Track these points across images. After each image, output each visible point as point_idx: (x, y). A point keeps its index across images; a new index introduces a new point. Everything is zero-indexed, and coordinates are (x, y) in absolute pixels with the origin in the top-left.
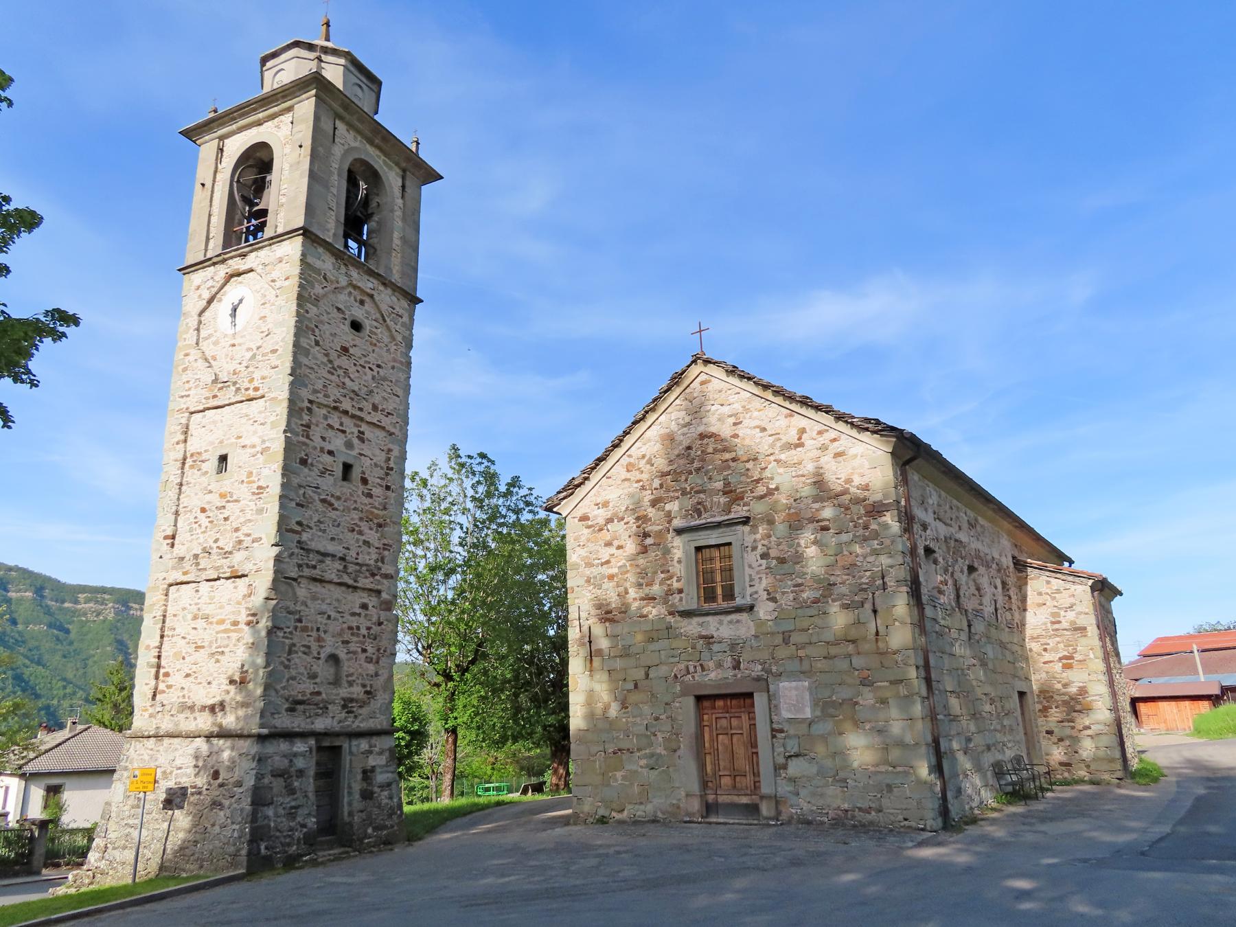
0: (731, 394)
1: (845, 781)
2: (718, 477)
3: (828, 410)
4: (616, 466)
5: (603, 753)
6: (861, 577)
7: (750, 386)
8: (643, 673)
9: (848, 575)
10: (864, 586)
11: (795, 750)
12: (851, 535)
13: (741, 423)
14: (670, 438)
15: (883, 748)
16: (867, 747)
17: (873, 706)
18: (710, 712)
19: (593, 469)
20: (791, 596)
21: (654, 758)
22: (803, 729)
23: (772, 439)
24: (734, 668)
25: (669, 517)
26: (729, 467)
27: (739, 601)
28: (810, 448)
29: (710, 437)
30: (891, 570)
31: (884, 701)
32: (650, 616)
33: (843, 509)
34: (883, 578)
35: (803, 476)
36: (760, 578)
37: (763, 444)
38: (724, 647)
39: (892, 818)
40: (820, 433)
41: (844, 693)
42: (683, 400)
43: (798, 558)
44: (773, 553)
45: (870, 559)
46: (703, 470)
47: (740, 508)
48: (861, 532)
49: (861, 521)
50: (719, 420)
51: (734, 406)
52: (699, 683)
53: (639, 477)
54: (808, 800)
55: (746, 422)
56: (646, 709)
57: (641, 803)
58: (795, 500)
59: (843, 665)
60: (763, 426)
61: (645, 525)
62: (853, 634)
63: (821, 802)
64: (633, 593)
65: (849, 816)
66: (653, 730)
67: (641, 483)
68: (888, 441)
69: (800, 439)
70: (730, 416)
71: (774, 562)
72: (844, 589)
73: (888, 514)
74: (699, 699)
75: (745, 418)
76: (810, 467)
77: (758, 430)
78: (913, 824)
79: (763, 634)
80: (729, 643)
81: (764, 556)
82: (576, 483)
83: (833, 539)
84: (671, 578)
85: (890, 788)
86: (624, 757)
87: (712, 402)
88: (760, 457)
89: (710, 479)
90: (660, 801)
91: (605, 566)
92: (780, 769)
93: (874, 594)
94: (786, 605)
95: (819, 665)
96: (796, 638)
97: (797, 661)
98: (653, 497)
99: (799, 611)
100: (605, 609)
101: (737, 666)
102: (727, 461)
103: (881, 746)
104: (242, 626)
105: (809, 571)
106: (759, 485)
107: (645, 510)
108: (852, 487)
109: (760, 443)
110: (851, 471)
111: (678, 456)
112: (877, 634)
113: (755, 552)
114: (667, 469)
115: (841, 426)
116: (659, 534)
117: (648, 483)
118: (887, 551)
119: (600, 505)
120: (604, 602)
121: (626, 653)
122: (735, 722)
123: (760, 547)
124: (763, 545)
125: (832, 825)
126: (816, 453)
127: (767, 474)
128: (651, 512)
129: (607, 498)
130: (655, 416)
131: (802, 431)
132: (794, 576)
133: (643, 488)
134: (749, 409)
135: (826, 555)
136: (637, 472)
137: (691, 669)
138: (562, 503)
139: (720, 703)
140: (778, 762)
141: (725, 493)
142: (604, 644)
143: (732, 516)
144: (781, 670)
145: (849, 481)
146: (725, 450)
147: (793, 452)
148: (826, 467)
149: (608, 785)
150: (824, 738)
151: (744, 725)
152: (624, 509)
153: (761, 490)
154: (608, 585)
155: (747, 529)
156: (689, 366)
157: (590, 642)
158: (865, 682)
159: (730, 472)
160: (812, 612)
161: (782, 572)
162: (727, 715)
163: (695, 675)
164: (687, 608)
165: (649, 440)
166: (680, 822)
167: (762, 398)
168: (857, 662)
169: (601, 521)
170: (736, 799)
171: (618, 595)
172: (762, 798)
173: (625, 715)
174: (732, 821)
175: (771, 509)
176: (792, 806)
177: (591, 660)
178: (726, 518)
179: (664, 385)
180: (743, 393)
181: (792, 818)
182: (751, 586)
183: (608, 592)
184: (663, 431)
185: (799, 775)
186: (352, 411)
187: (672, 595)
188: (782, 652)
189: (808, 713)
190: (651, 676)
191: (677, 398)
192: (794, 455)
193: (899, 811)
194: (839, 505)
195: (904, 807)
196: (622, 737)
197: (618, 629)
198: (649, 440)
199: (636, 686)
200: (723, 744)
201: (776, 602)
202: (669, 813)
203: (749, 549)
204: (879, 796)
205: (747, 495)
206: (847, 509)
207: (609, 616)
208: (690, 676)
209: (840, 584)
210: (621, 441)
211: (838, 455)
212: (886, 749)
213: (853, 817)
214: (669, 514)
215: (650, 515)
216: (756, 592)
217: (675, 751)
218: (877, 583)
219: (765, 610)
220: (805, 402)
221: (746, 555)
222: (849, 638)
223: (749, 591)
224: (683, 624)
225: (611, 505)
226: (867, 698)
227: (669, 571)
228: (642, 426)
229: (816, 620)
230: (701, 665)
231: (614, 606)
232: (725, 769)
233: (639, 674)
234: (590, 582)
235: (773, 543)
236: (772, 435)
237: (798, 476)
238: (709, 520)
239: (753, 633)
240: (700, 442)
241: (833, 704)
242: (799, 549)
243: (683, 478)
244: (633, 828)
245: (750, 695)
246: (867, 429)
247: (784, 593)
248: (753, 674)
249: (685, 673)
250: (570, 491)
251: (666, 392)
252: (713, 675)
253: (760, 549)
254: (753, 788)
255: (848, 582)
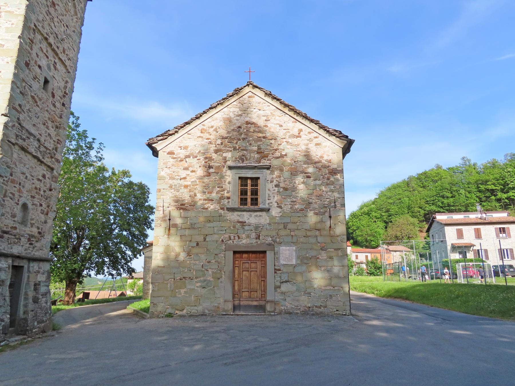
0: (265, 106)
1: (310, 293)
2: (255, 144)
3: (317, 123)
4: (195, 129)
5: (173, 280)
6: (324, 201)
7: (277, 104)
8: (203, 238)
9: (318, 199)
10: (326, 205)
11: (286, 279)
12: (321, 182)
13: (269, 120)
14: (229, 120)
15: (329, 279)
16: (322, 278)
17: (326, 259)
18: (239, 260)
19: (182, 127)
20: (290, 206)
21: (205, 283)
22: (291, 269)
23: (285, 131)
24: (256, 239)
25: (225, 160)
26: (261, 141)
27: (261, 206)
28: (304, 139)
29: (252, 124)
30: (339, 200)
31: (331, 258)
32: (209, 209)
33: (318, 169)
34: (335, 203)
35: (299, 151)
36: (274, 196)
37: (280, 133)
38: (252, 228)
39: (331, 310)
40: (309, 133)
41: (313, 253)
42: (238, 103)
43: (294, 189)
44: (282, 185)
45: (330, 193)
46: (247, 140)
47: (266, 161)
48: (326, 181)
49: (326, 176)
50: (258, 117)
51: (266, 112)
52: (236, 245)
53: (208, 137)
54: (290, 303)
55: (272, 121)
56: (203, 257)
57: (196, 306)
58: (295, 162)
59: (312, 240)
60: (281, 124)
61: (210, 162)
62: (319, 226)
63: (297, 304)
64: (199, 196)
65: (311, 310)
66: (206, 268)
67: (210, 140)
68: (343, 142)
69: (299, 134)
70: (263, 116)
71: (282, 190)
72: (316, 206)
73: (339, 175)
74: (235, 253)
75: (271, 118)
76: (303, 148)
77: (278, 126)
78: (341, 313)
79: (273, 223)
80: (255, 226)
81: (276, 186)
82: (170, 133)
83: (312, 183)
84: (224, 190)
85: (331, 296)
86: (187, 282)
87: (255, 107)
88: (278, 139)
89: (250, 144)
90: (207, 304)
91: (183, 180)
92: (277, 288)
93: (330, 209)
94: (287, 210)
95: (301, 240)
96: (290, 226)
97: (290, 237)
98: (216, 148)
99: (293, 214)
100: (181, 203)
101: (258, 237)
102: (260, 137)
103: (328, 278)
104: (96, 149)
105: (299, 195)
106: (277, 152)
107: (211, 155)
108: (323, 160)
109: (278, 132)
110: (323, 153)
111: (233, 130)
112: (330, 227)
113: (272, 184)
114: (225, 135)
115: (321, 132)
116: (218, 168)
117: (214, 141)
118: (337, 191)
119: (182, 148)
120: (180, 199)
121: (192, 227)
122: (253, 265)
123: (275, 181)
124: (277, 181)
125: (302, 314)
126: (307, 142)
127: (281, 147)
128: (214, 156)
129: (187, 144)
130: (222, 108)
131: (301, 130)
132: (291, 197)
133: (210, 143)
134: (274, 115)
135: (308, 189)
136: (208, 134)
137: (232, 238)
138: (159, 143)
139: (245, 255)
140: (277, 285)
141: (258, 153)
142: (179, 221)
143: (261, 164)
144: (282, 241)
145: (322, 157)
146: (260, 132)
147: (295, 139)
148: (311, 149)
149: (175, 296)
150: (301, 273)
151: (258, 267)
152: (197, 152)
153: (277, 154)
154: (183, 190)
155: (268, 172)
156: (245, 87)
157: (170, 220)
158: (322, 249)
159: (262, 143)
160: (299, 215)
161: (285, 194)
162: (249, 262)
163: (235, 241)
164: (232, 207)
165: (216, 119)
166: (219, 315)
167: (281, 111)
168: (320, 239)
169: (182, 156)
170: (251, 303)
171: (190, 196)
172: (268, 302)
173: (189, 260)
174: (250, 314)
175: (282, 164)
176: (282, 306)
177: (169, 229)
178: (258, 165)
179: (231, 93)
180: (271, 106)
181: (282, 311)
182: (268, 199)
183: (183, 194)
184: (225, 116)
185: (287, 291)
186: (54, 46)
187: (223, 199)
188: (283, 233)
189: (294, 262)
190: (207, 240)
191: (235, 101)
192: (295, 141)
193: (334, 307)
194: (316, 167)
195: (337, 305)
196: (186, 271)
197: (190, 214)
198: (216, 119)
199: (198, 244)
200: (245, 275)
201: (281, 209)
202: (212, 310)
203: (269, 182)
204: (326, 300)
205: (270, 155)
206: (320, 170)
207: (182, 207)
208: (231, 241)
209: (314, 203)
210: (201, 116)
211: (317, 144)
212: (330, 279)
213: (313, 310)
214: (225, 158)
215: (214, 157)
216: (271, 203)
217: (219, 279)
218: (332, 205)
219: (275, 212)
220: (306, 117)
221: (267, 184)
222: (317, 228)
223: (268, 202)
224: (228, 215)
225: (189, 149)
226: (324, 255)
227: (222, 187)
228: (214, 111)
229: (302, 219)
230: (238, 236)
231: (186, 201)
232: (245, 288)
233: (200, 239)
234: (171, 187)
235: (282, 180)
236: (285, 129)
237: (297, 151)
238: (248, 165)
239: (268, 222)
240: (246, 126)
241: (307, 258)
242: (295, 185)
243: (235, 142)
244: (196, 318)
245: (264, 252)
246: (334, 135)
247: (285, 205)
248: (267, 242)
249: (228, 239)
250: (166, 137)
251: (230, 96)
252: (244, 241)
253: (275, 182)
254: (260, 297)
255: (318, 203)
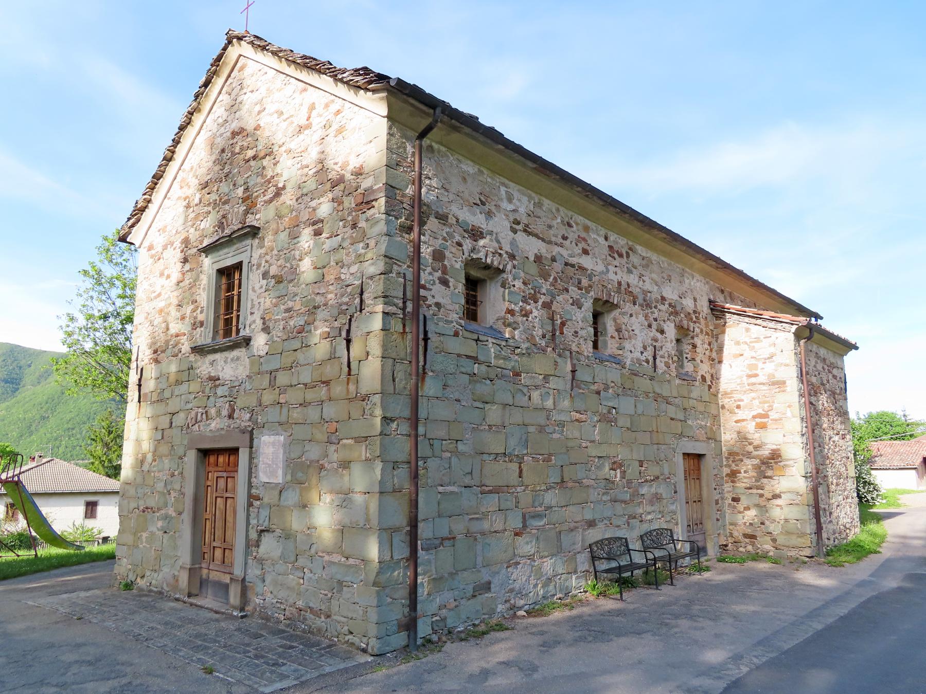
74: (205, 453)
76: (313, 155)
78: (356, 640)
96: (283, 379)
101: (231, 416)
145: (346, 164)
156: (225, 49)
189: (279, 478)
191: (220, 93)
193: (345, 620)
195: (350, 616)
219: (260, 342)
245: (235, 451)
252: (213, 425)
